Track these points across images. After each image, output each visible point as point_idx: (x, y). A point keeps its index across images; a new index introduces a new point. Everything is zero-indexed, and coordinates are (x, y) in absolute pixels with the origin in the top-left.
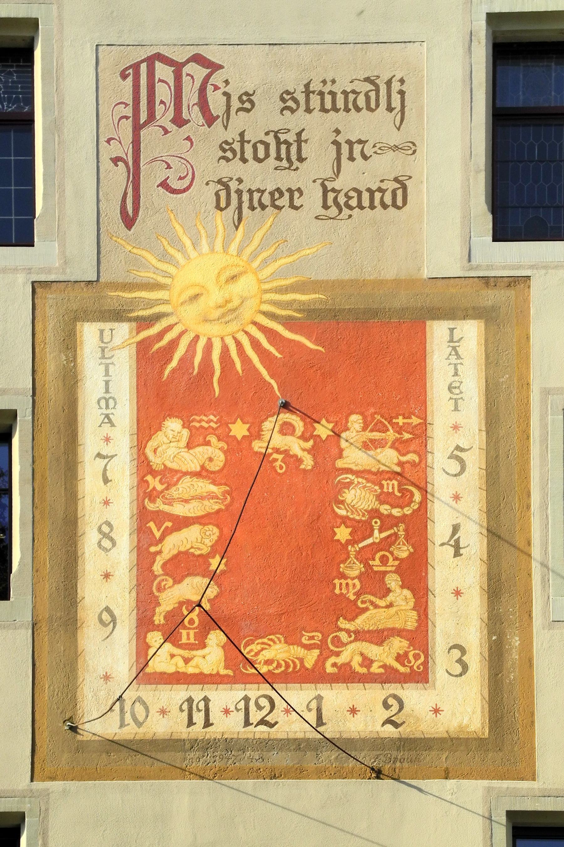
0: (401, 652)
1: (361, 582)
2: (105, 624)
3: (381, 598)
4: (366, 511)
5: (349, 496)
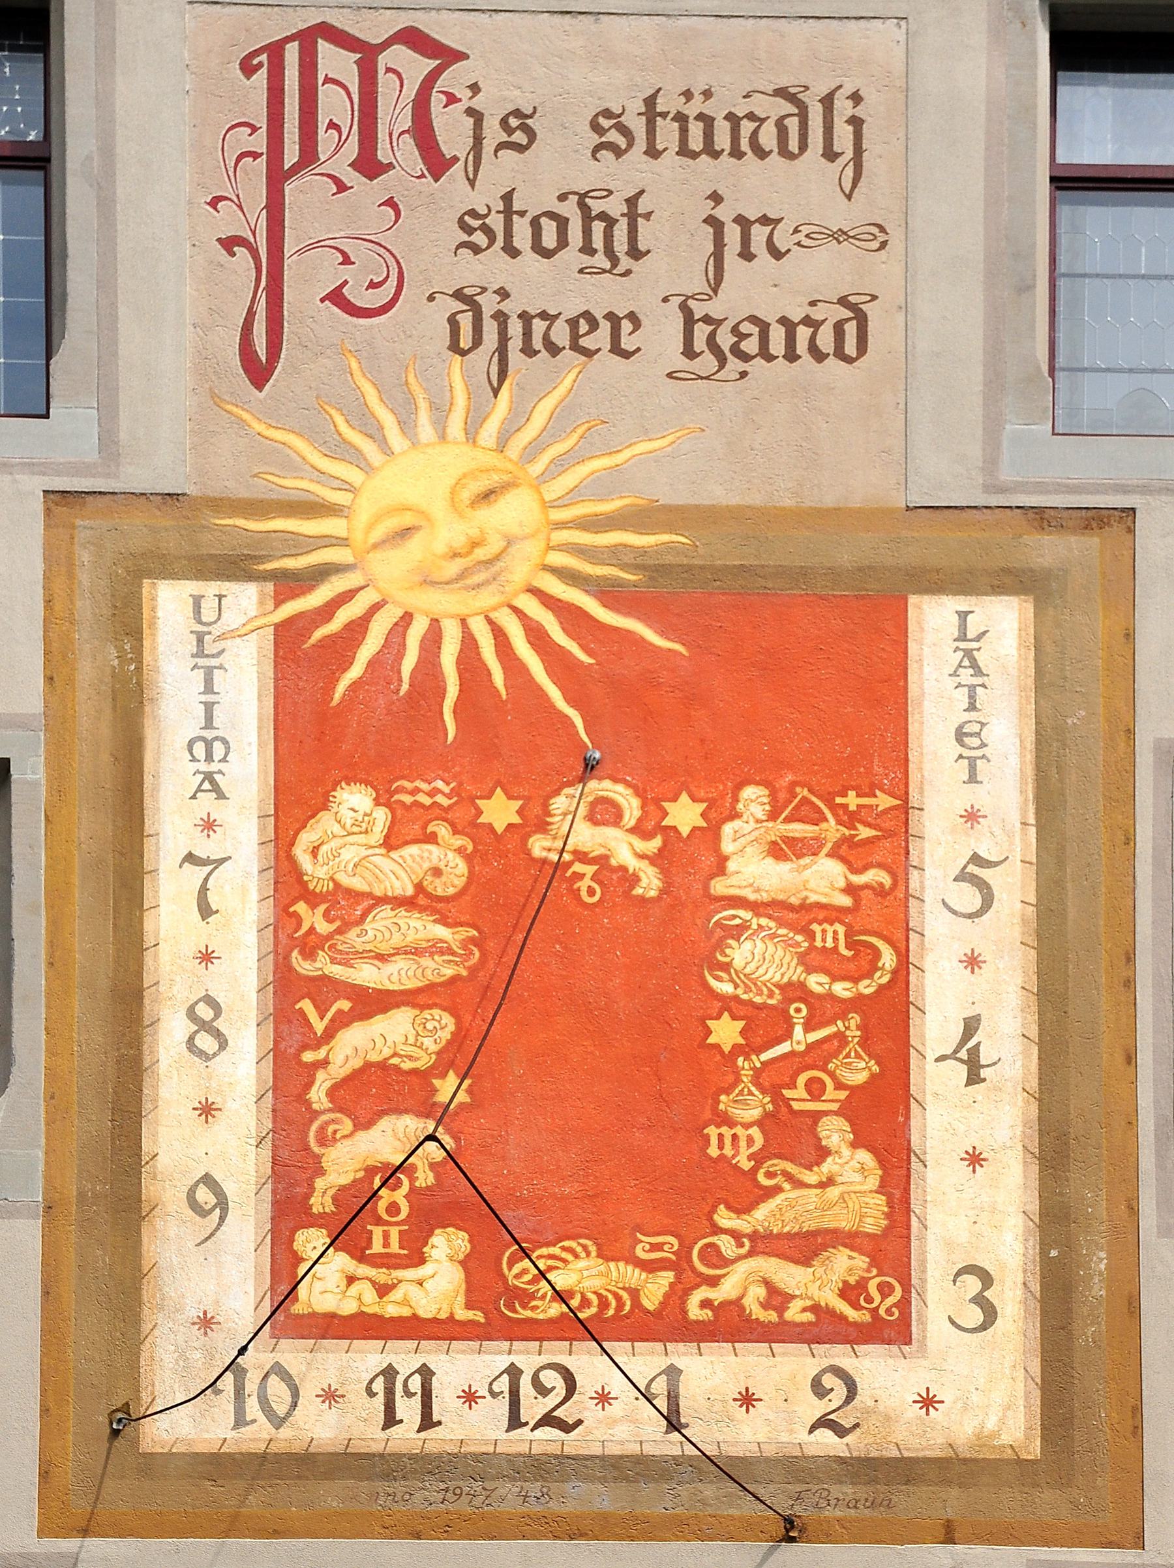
0: (852, 1280)
1: (763, 1132)
2: (204, 1210)
3: (809, 1168)
4: (777, 985)
5: (740, 954)
